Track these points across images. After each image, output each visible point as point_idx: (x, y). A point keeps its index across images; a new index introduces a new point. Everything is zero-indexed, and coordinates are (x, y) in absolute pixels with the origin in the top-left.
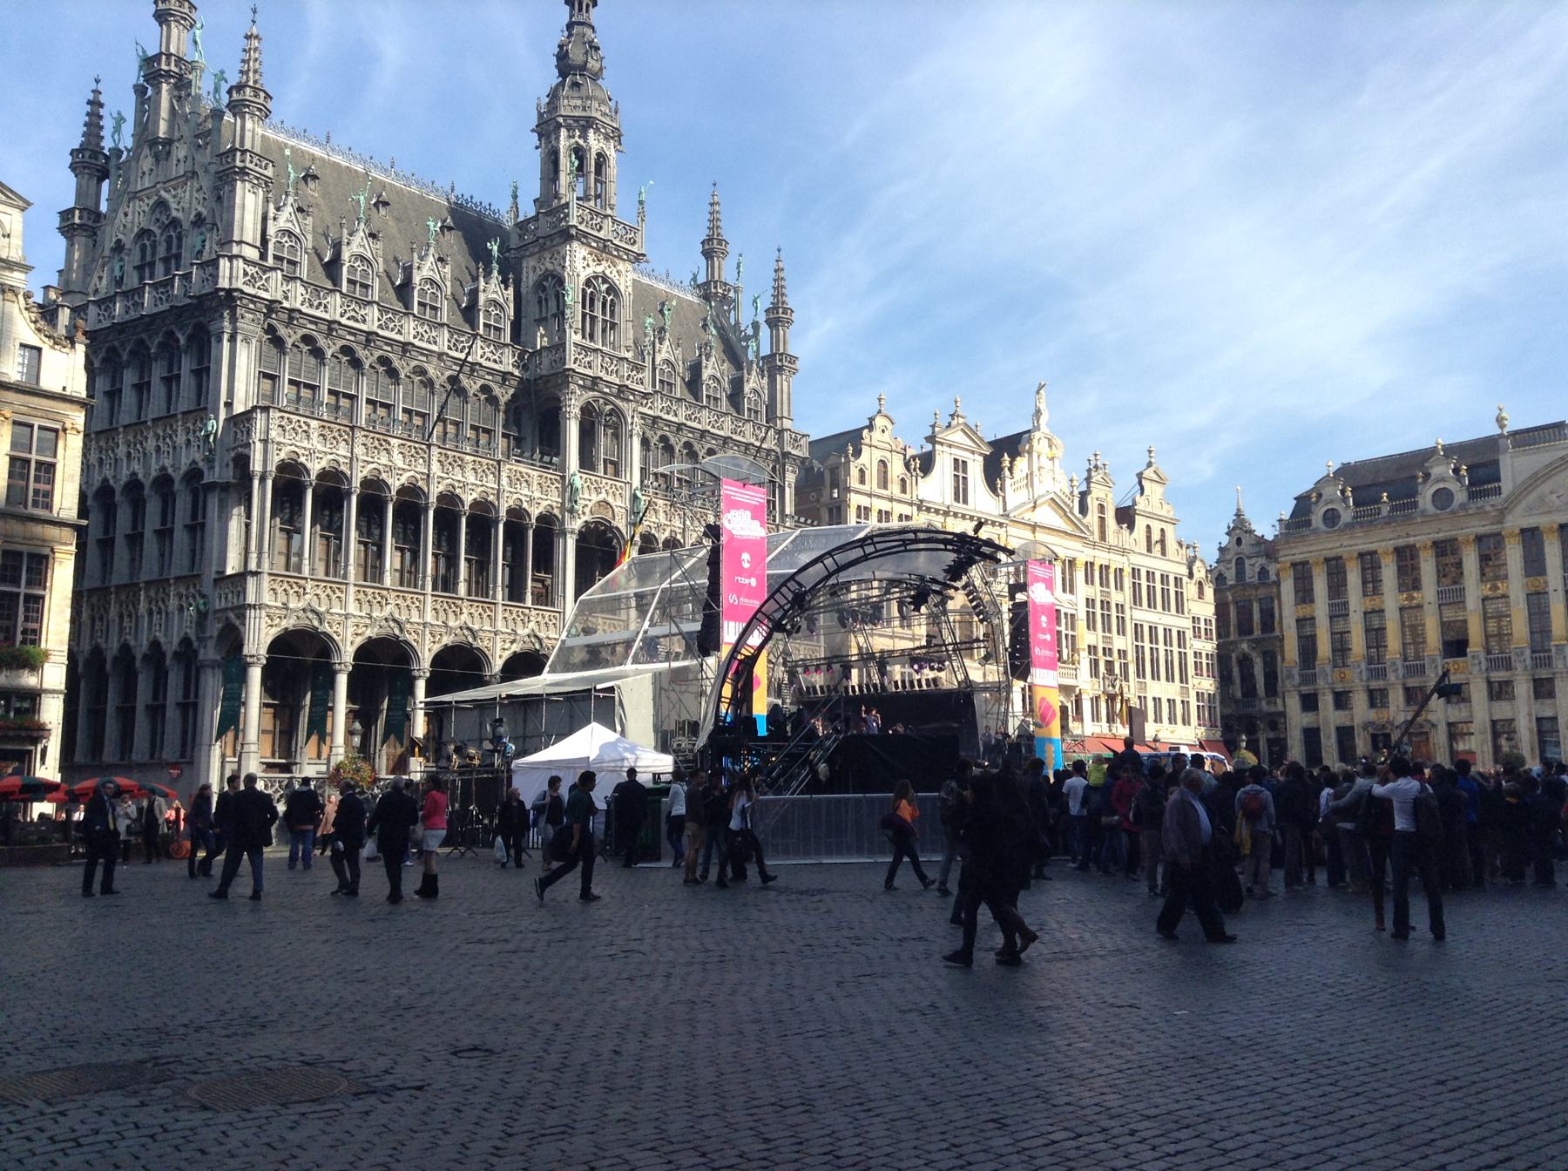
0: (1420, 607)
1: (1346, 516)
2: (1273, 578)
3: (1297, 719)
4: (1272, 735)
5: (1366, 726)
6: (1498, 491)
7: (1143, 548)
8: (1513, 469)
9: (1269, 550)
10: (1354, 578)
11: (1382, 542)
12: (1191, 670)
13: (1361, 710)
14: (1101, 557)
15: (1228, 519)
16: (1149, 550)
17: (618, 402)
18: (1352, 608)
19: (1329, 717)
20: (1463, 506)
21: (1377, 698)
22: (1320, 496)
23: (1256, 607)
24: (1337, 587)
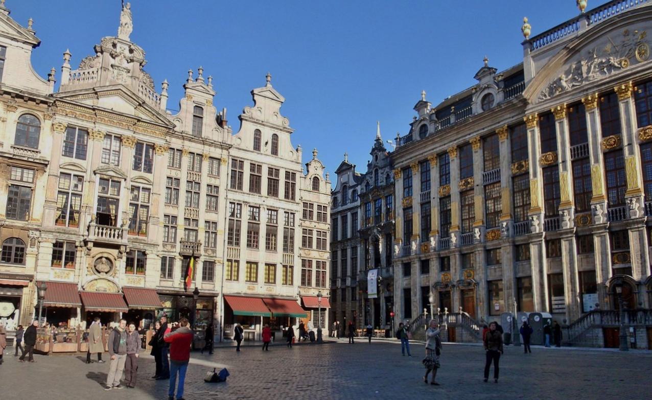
1: (431, 129)
2: (392, 180)
4: (387, 294)
5: (436, 284)
7: (251, 146)
9: (391, 159)
10: (434, 174)
11: (449, 144)
12: (298, 242)
13: (435, 273)
14: (196, 148)
15: (372, 144)
16: (257, 147)
18: (432, 196)
19: (417, 279)
20: (499, 105)
21: (444, 265)
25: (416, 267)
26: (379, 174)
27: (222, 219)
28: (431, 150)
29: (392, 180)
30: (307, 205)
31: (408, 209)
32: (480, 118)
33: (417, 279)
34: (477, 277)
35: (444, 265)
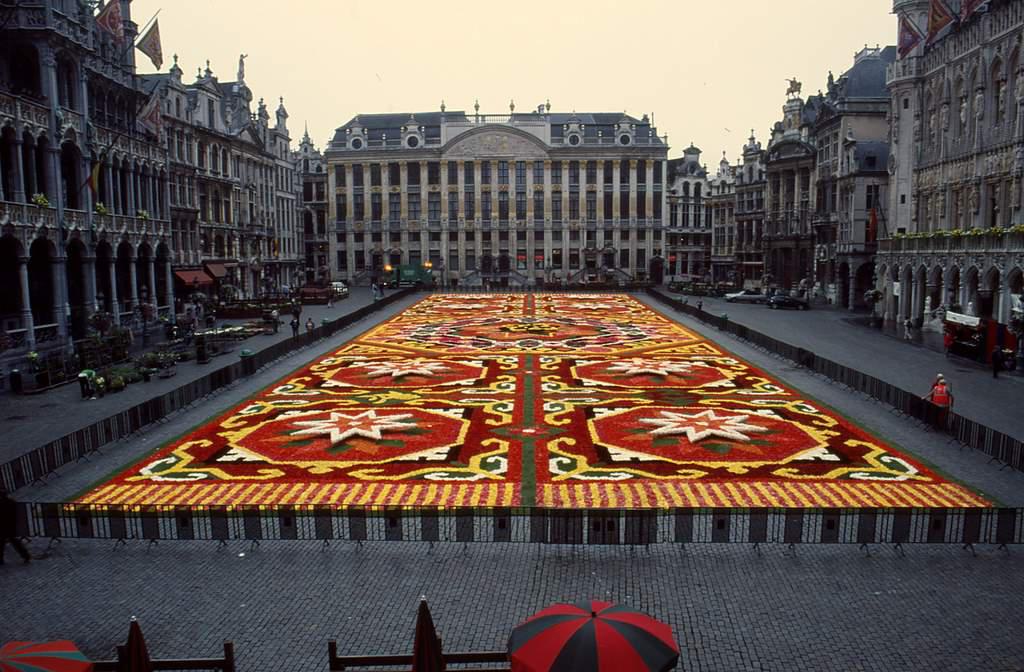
0: (399, 194)
1: (364, 145)
3: (335, 246)
4: (321, 254)
6: (439, 142)
8: (447, 132)
10: (367, 177)
13: (368, 243)
17: (73, 55)
21: (377, 237)
22: (351, 131)
23: (314, 186)
24: (358, 180)
25: (351, 238)
26: (310, 165)
27: (272, 209)
28: (366, 161)
29: (324, 172)
30: (297, 194)
31: (341, 197)
32: (407, 152)
33: (352, 245)
34: (402, 249)
35: (377, 237)
